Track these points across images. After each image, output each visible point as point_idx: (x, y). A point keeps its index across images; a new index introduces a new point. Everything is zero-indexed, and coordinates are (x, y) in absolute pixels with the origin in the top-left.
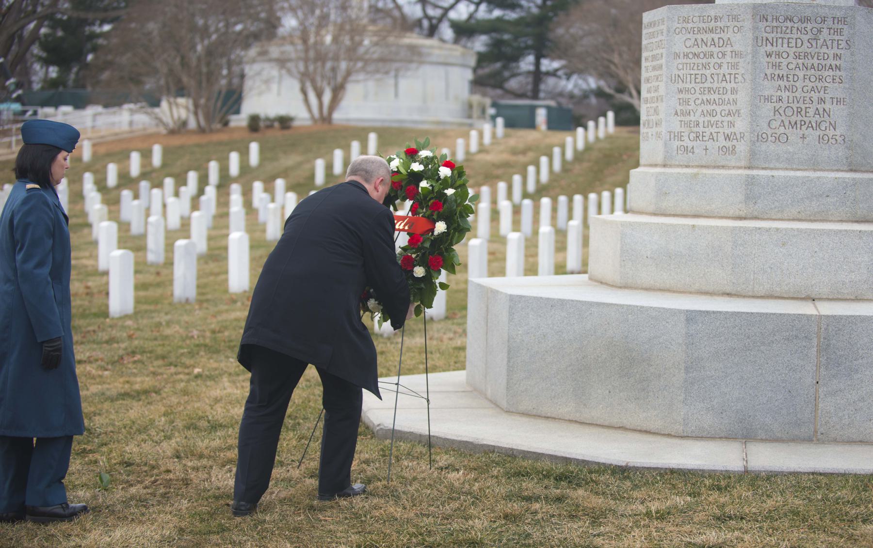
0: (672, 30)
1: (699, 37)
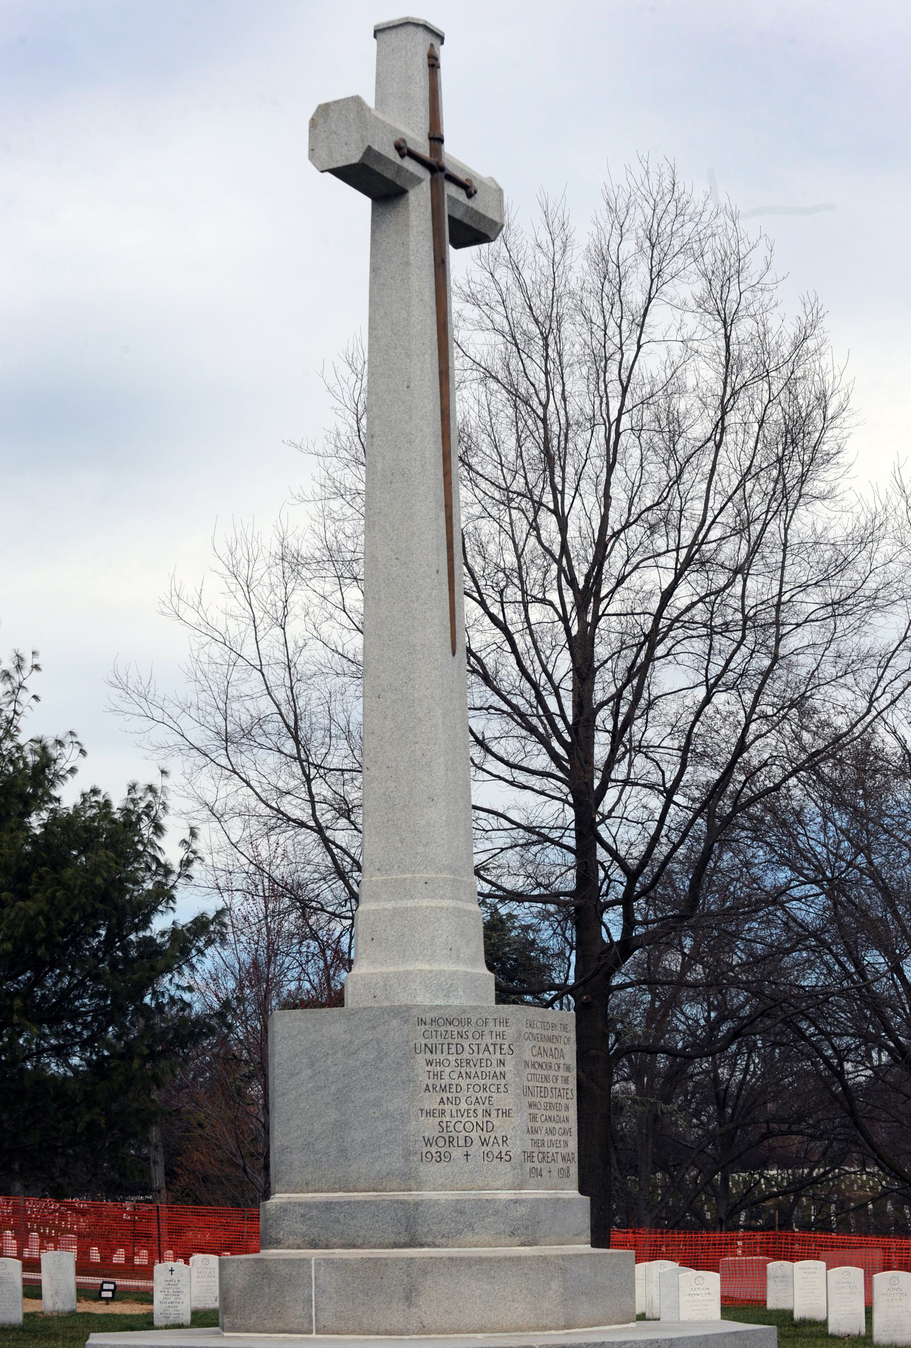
0: (522, 1034)
1: (541, 1044)
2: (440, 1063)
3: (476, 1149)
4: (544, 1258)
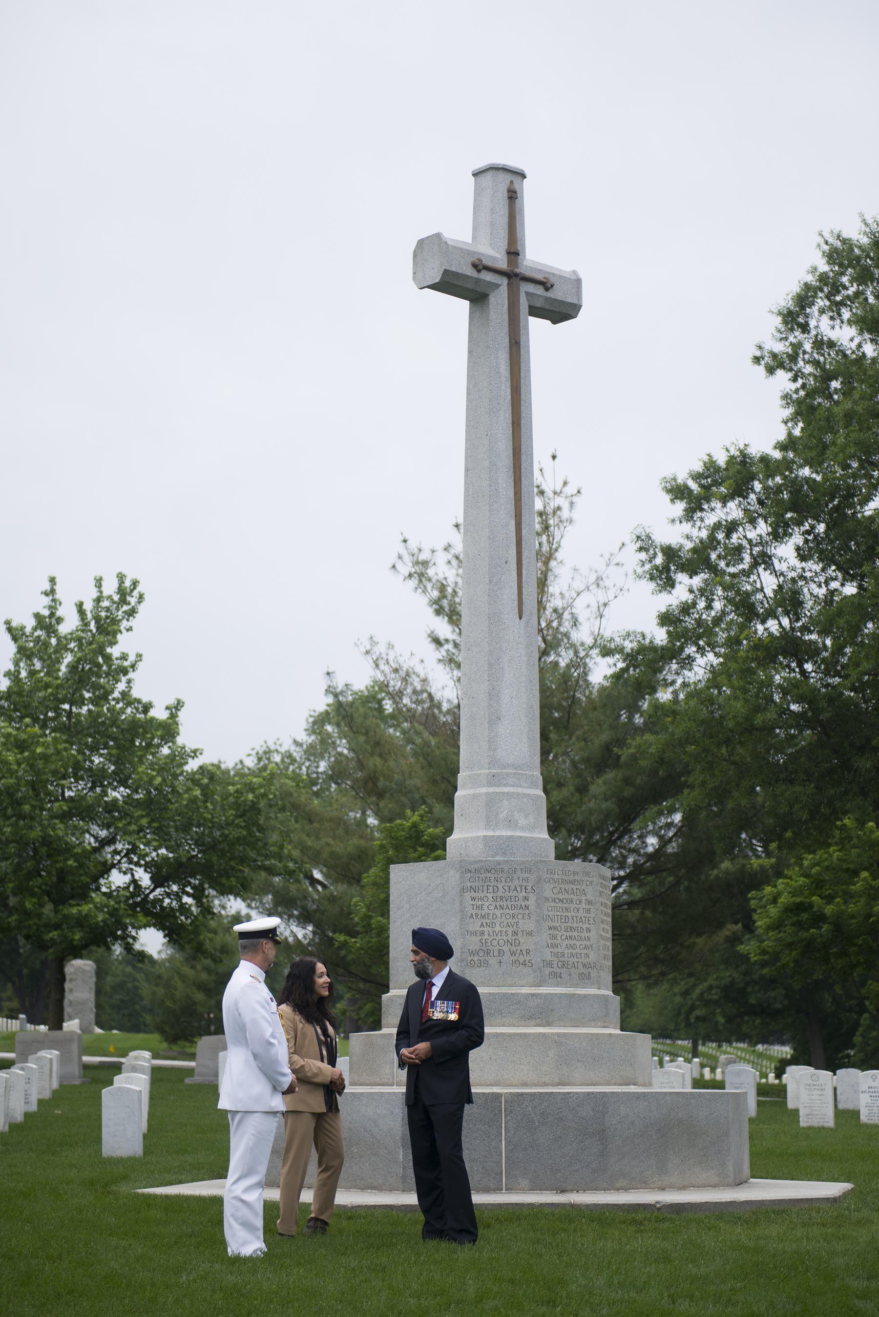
1: (563, 886)
2: (481, 899)
3: (507, 958)
4: (544, 1035)
